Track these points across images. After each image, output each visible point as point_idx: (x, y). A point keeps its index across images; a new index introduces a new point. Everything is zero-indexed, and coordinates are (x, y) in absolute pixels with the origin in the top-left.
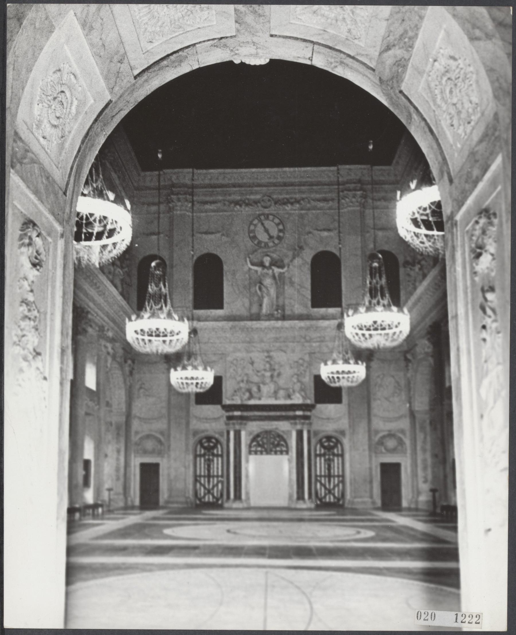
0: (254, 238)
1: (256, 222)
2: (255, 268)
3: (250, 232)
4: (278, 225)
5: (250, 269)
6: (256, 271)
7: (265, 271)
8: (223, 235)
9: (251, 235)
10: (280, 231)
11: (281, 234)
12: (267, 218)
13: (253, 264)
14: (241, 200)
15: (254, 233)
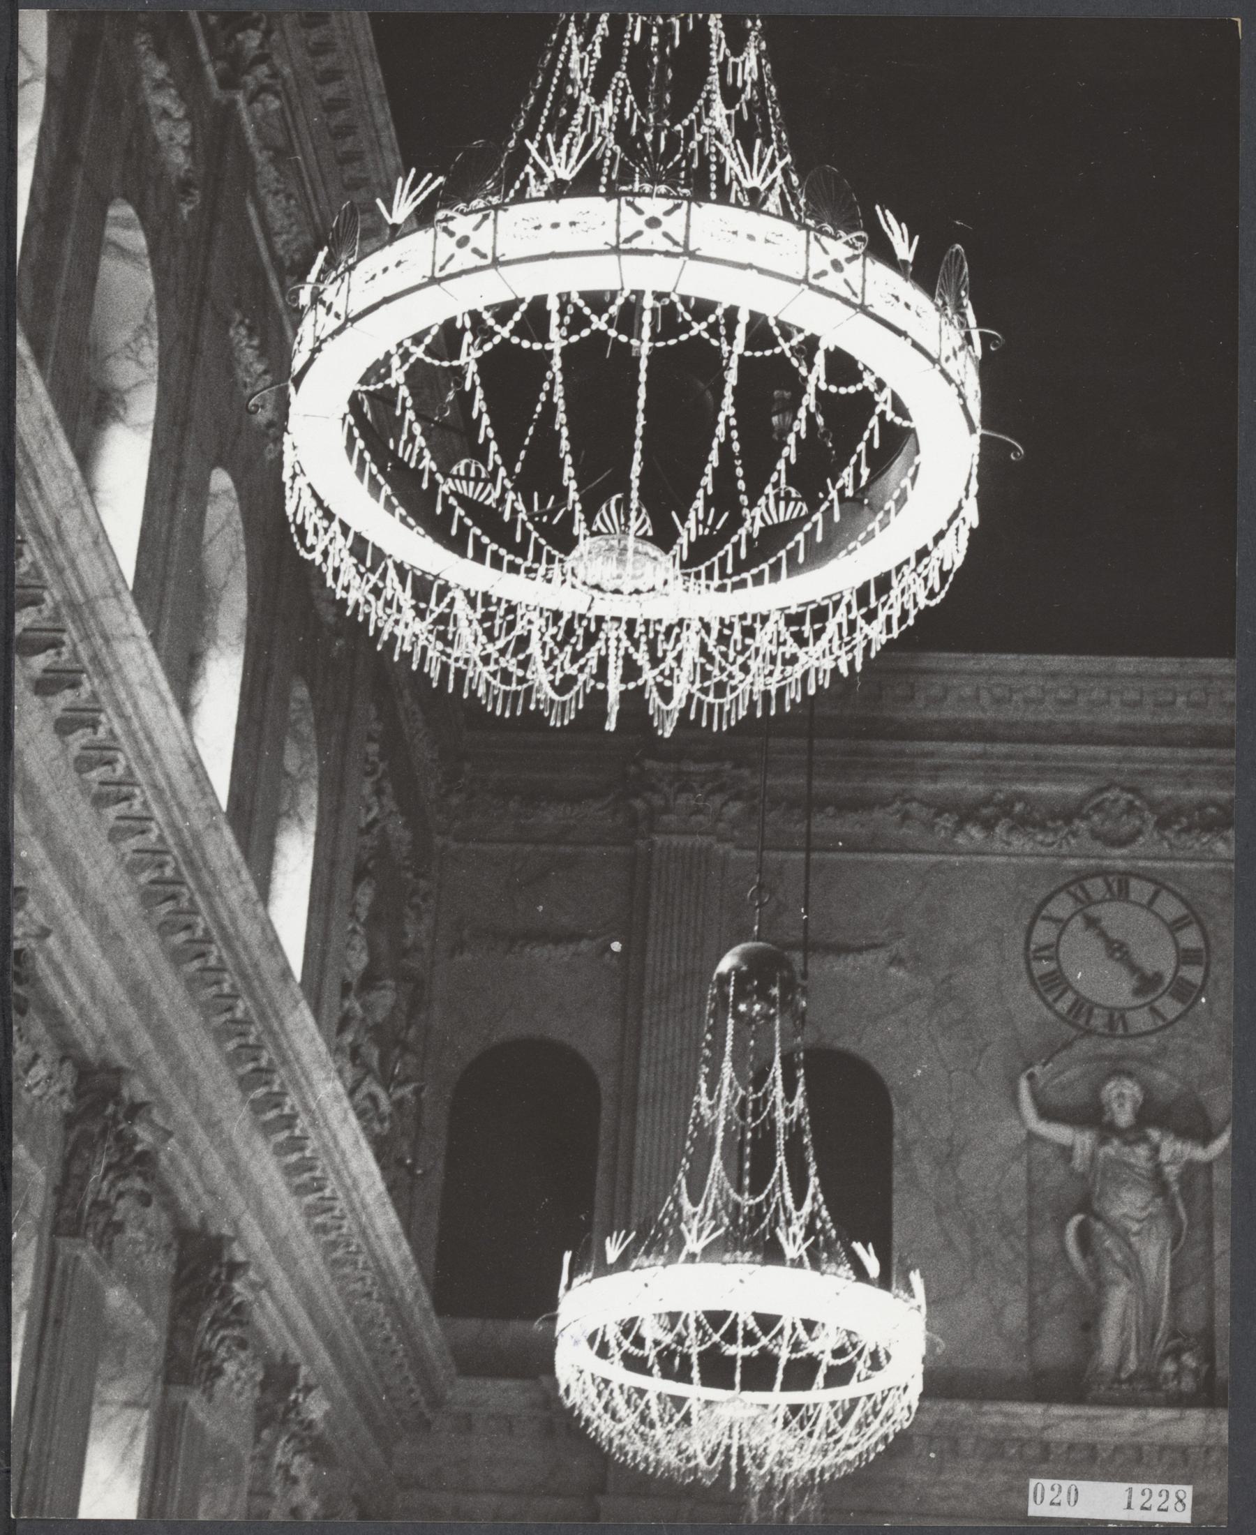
0: (1055, 982)
1: (1062, 907)
2: (1061, 1133)
3: (1030, 956)
4: (1175, 927)
5: (1032, 1137)
6: (1066, 1152)
7: (1111, 1149)
8: (896, 961)
9: (1045, 966)
10: (1186, 957)
11: (1194, 974)
12: (1122, 894)
13: (1047, 1113)
14: (987, 801)
15: (1055, 958)
